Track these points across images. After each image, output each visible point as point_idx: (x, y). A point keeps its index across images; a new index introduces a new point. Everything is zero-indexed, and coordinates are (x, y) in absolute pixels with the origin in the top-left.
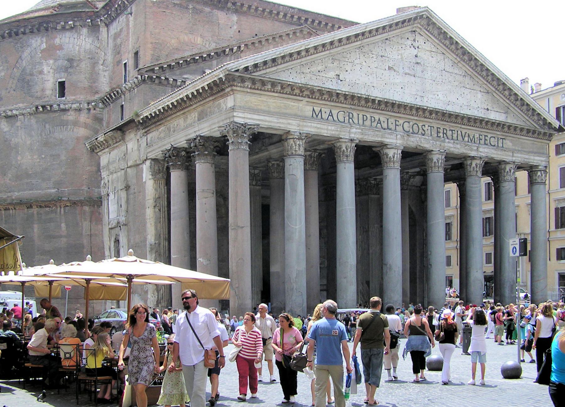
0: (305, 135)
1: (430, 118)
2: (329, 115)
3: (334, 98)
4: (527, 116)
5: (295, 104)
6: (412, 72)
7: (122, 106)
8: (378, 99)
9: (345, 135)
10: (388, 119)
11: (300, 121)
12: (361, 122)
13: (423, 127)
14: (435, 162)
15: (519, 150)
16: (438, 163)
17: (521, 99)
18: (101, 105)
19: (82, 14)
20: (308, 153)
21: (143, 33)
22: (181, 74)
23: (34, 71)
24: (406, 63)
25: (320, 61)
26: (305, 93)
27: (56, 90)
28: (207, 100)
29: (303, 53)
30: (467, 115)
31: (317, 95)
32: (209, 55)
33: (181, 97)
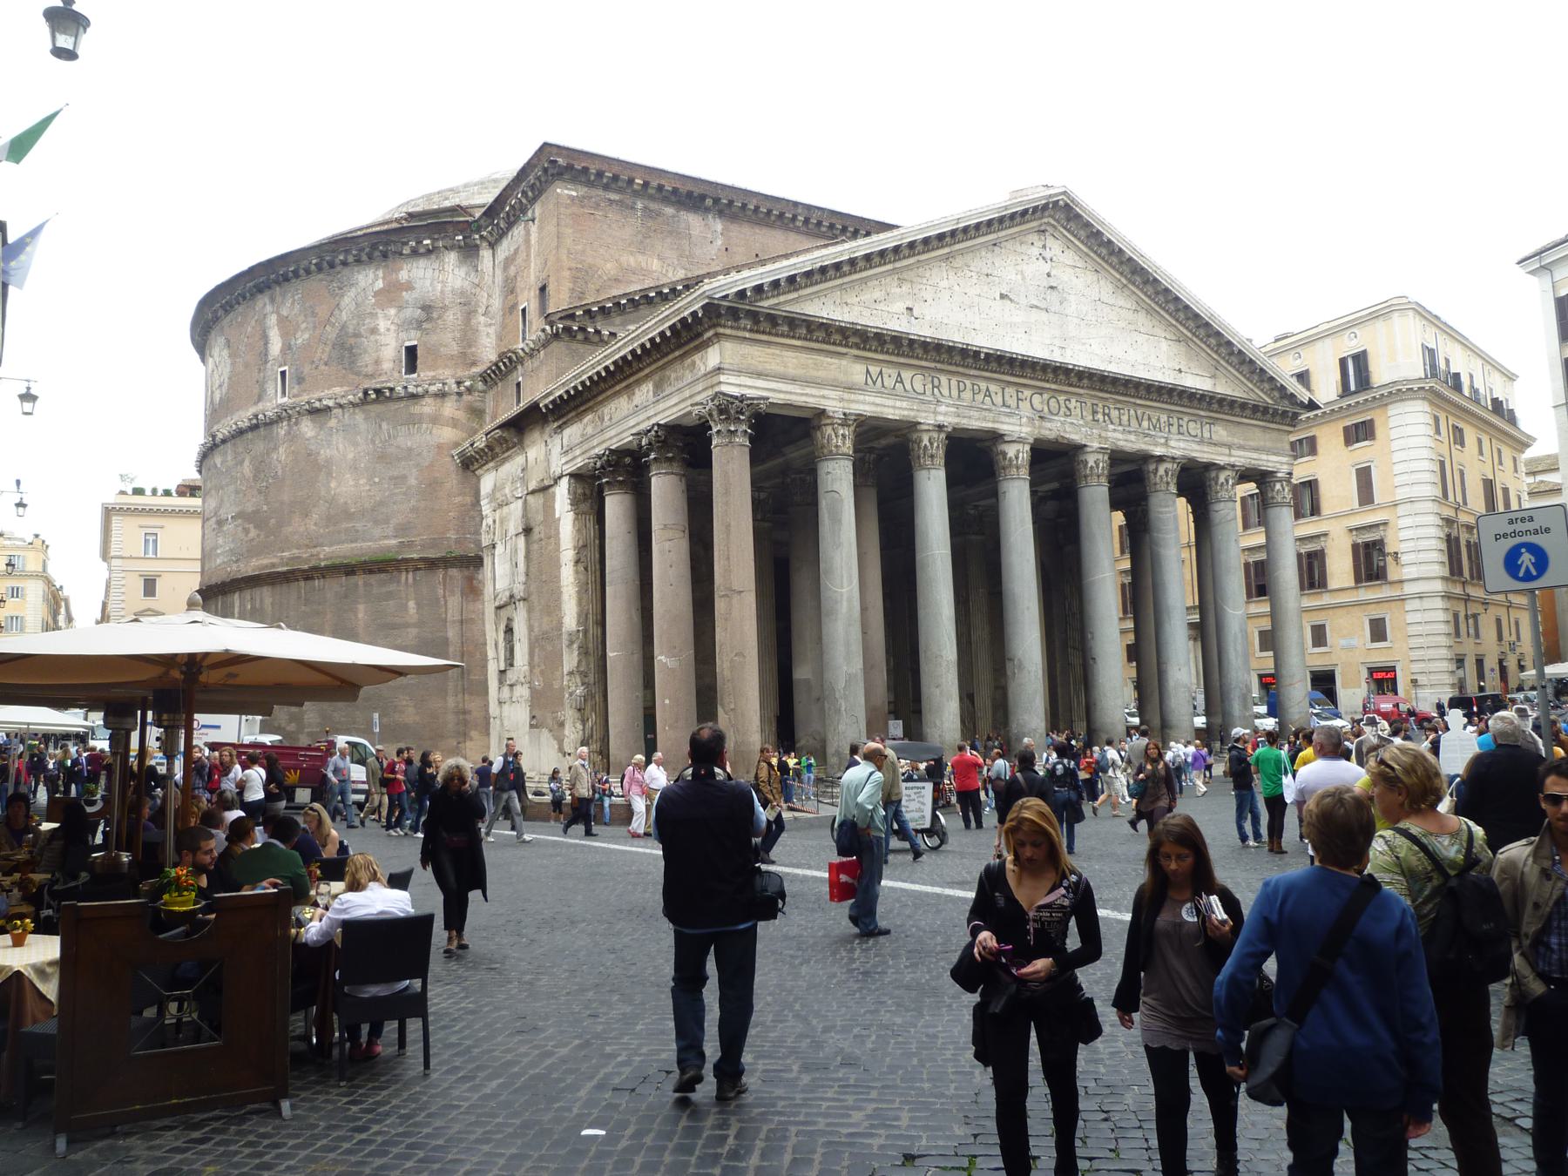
0: (853, 417)
1: (1079, 387)
2: (896, 381)
3: (905, 349)
4: (1251, 382)
5: (833, 360)
7: (518, 385)
9: (927, 419)
10: (1003, 389)
12: (955, 393)
14: (1092, 467)
16: (1098, 468)
17: (1240, 351)
18: (480, 385)
19: (448, 226)
20: (859, 455)
21: (554, 252)
22: (624, 324)
23: (362, 330)
24: (1031, 288)
26: (852, 340)
27: (401, 362)
28: (671, 357)
29: (846, 268)
31: (874, 344)
32: (673, 290)
33: (622, 353)
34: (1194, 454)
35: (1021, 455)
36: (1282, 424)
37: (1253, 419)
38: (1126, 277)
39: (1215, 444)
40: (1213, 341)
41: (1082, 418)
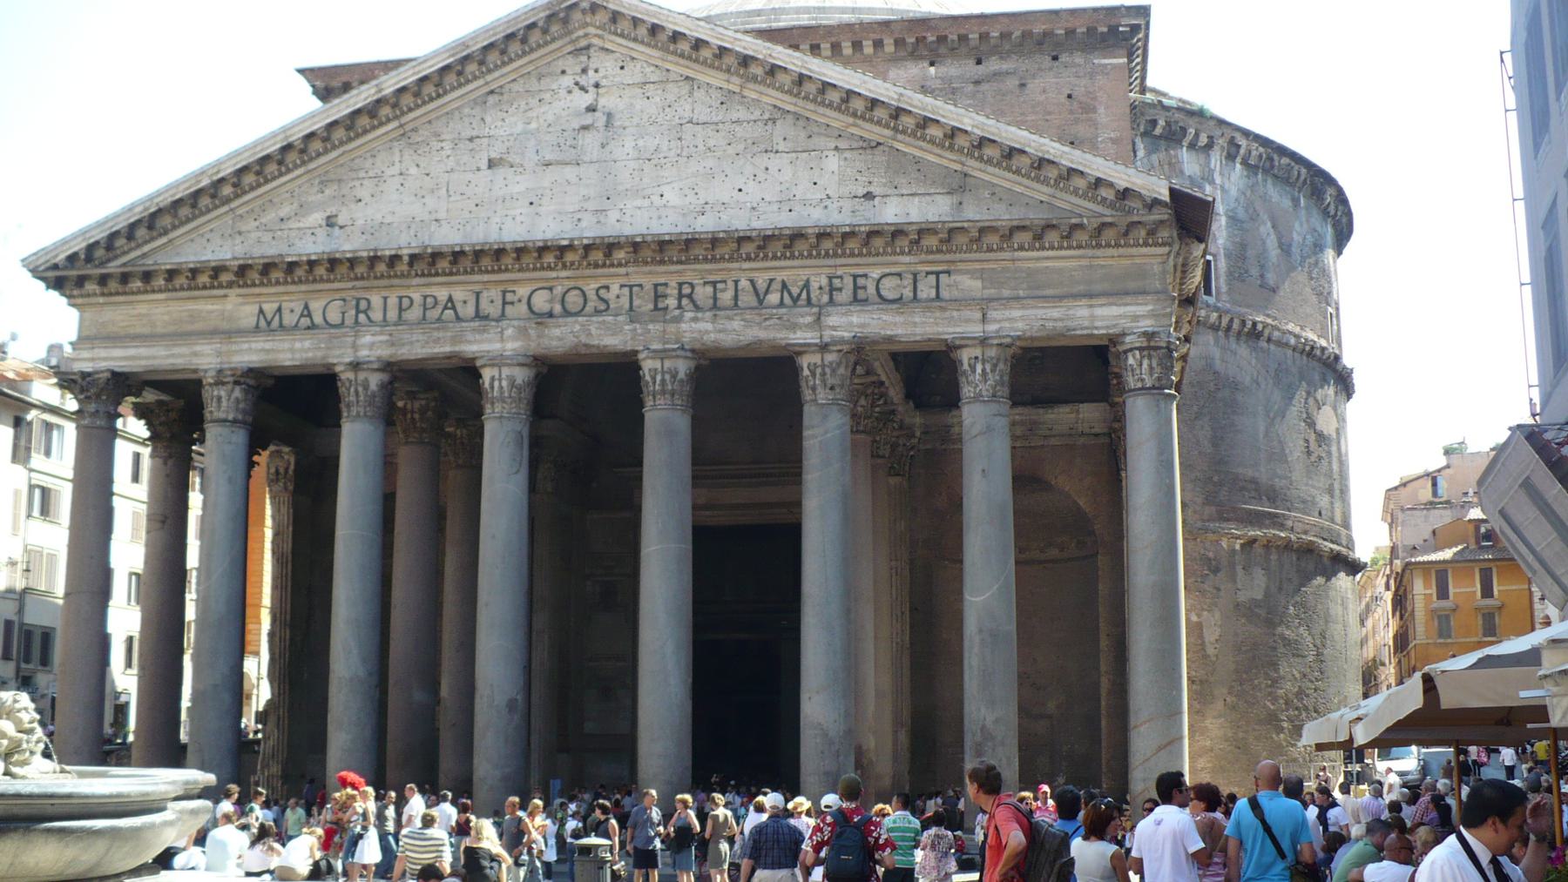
0: (229, 373)
1: (612, 265)
2: (302, 315)
4: (1046, 182)
5: (215, 307)
6: (570, 155)
8: (405, 252)
9: (339, 356)
10: (478, 294)
11: (221, 343)
12: (392, 314)
13: (602, 292)
15: (1009, 299)
16: (654, 383)
25: (288, 195)
30: (725, 231)
34: (889, 333)
35: (496, 384)
36: (1127, 245)
37: (1043, 248)
38: (738, 75)
39: (943, 309)
40: (933, 131)
41: (631, 308)
